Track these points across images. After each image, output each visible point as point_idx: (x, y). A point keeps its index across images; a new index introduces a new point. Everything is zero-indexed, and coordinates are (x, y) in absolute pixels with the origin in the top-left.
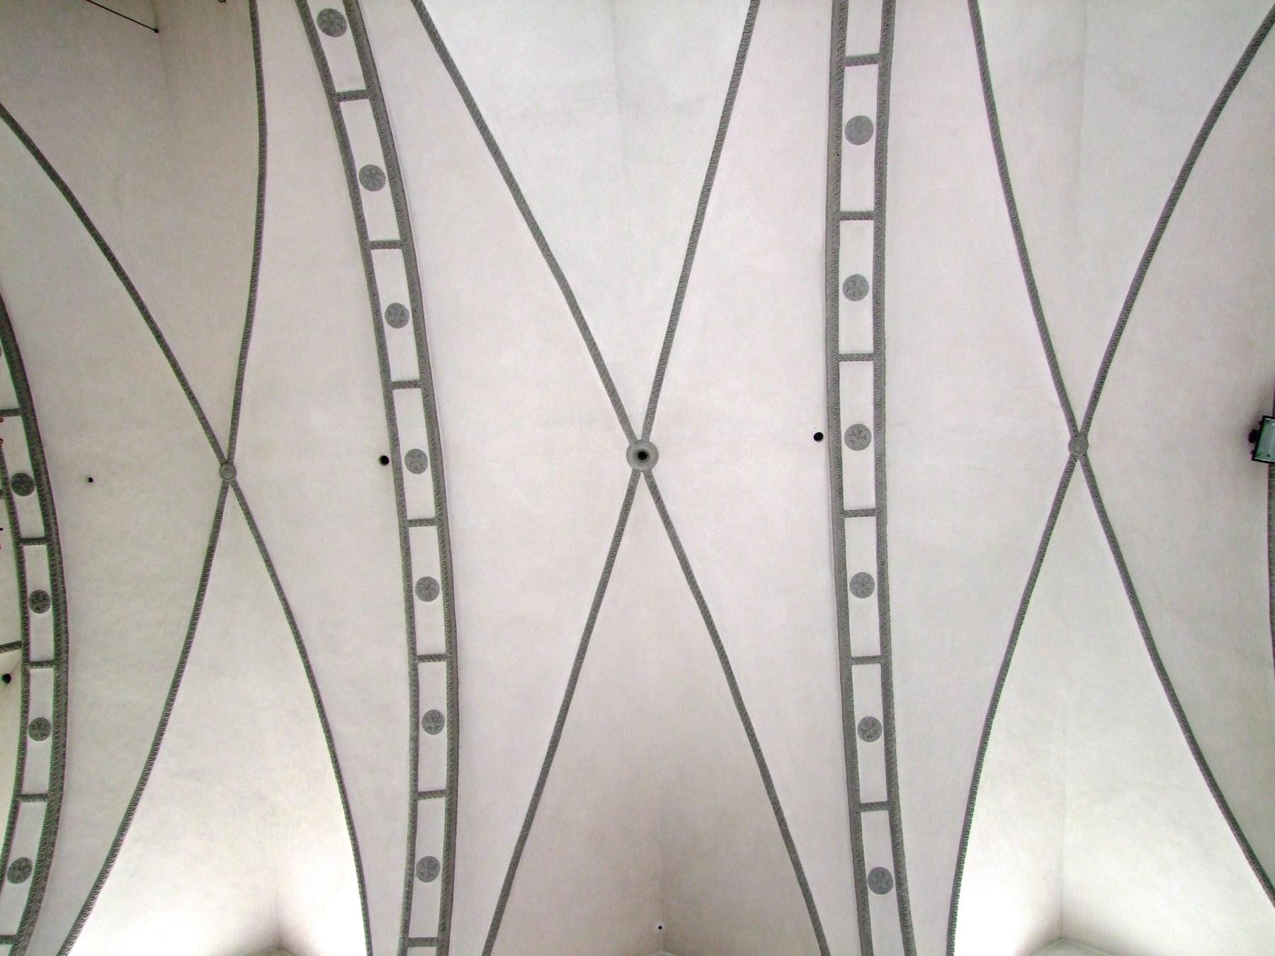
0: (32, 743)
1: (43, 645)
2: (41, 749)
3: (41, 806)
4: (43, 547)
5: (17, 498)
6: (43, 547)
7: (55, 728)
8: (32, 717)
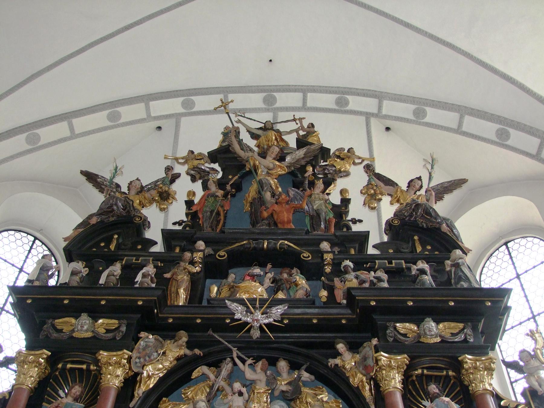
0: (427, 119)
1: (369, 105)
2: (432, 115)
3: (467, 119)
4: (309, 95)
5: (278, 105)
6: (309, 95)
7: (421, 105)
8: (411, 117)
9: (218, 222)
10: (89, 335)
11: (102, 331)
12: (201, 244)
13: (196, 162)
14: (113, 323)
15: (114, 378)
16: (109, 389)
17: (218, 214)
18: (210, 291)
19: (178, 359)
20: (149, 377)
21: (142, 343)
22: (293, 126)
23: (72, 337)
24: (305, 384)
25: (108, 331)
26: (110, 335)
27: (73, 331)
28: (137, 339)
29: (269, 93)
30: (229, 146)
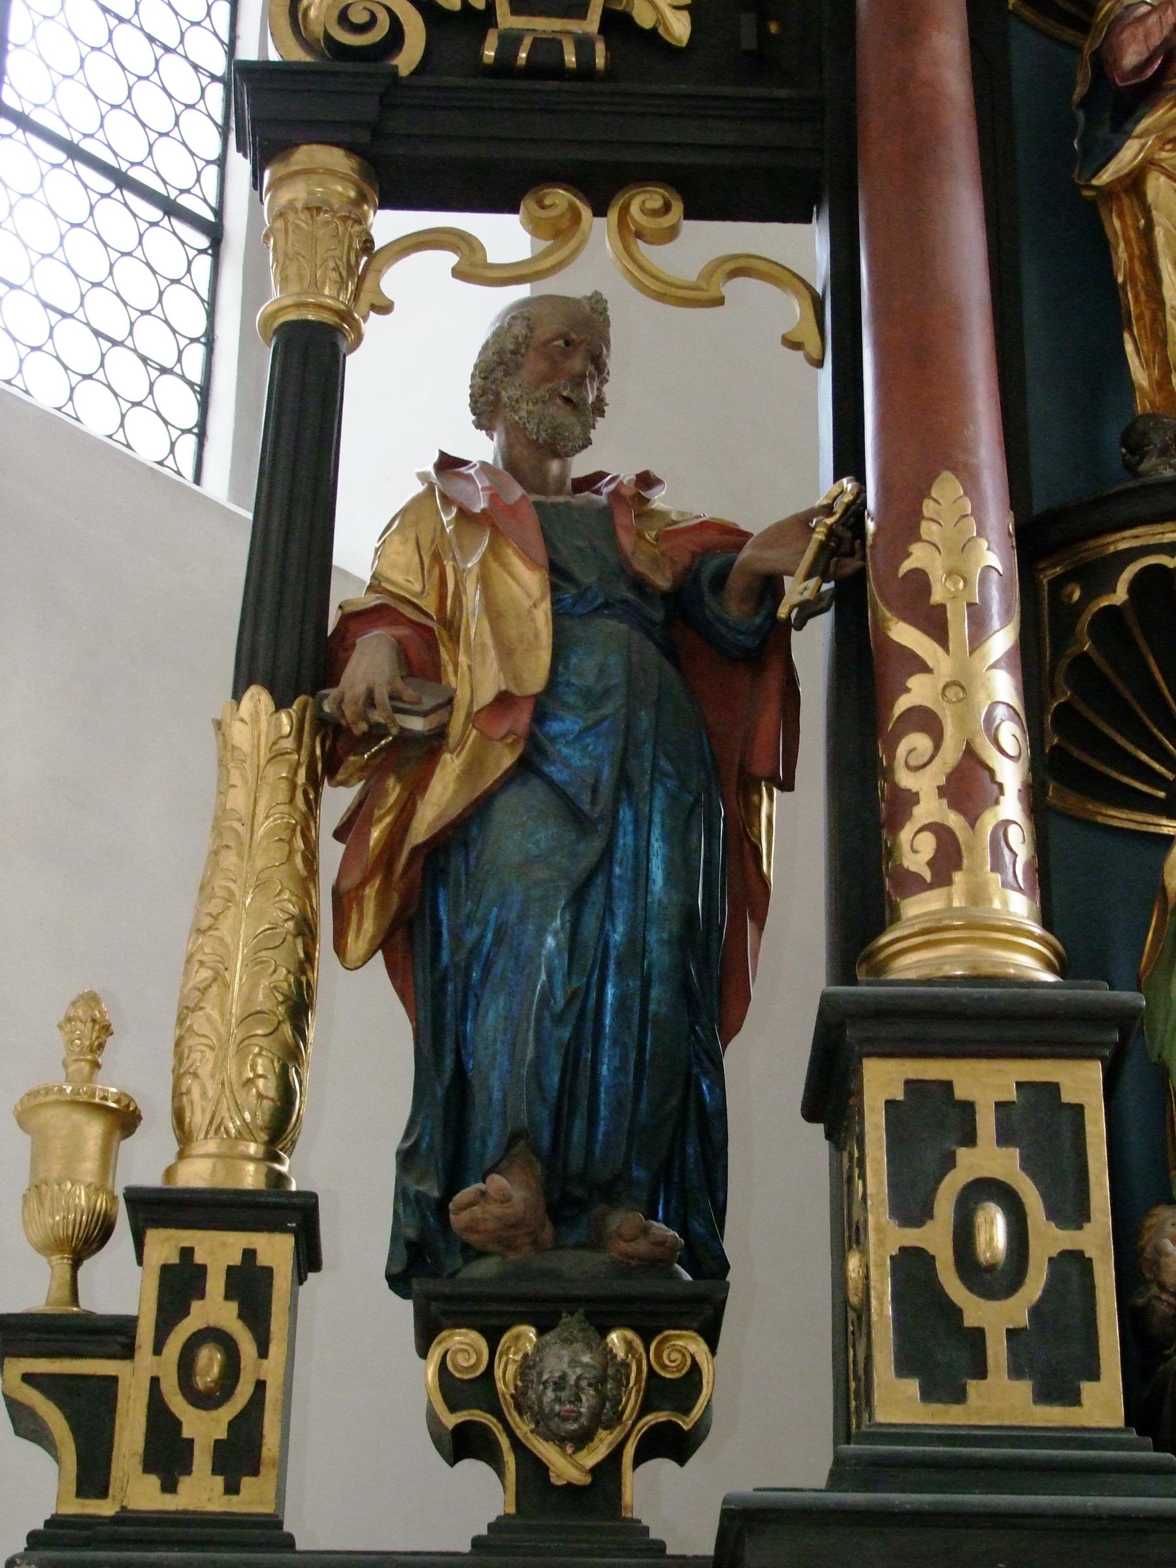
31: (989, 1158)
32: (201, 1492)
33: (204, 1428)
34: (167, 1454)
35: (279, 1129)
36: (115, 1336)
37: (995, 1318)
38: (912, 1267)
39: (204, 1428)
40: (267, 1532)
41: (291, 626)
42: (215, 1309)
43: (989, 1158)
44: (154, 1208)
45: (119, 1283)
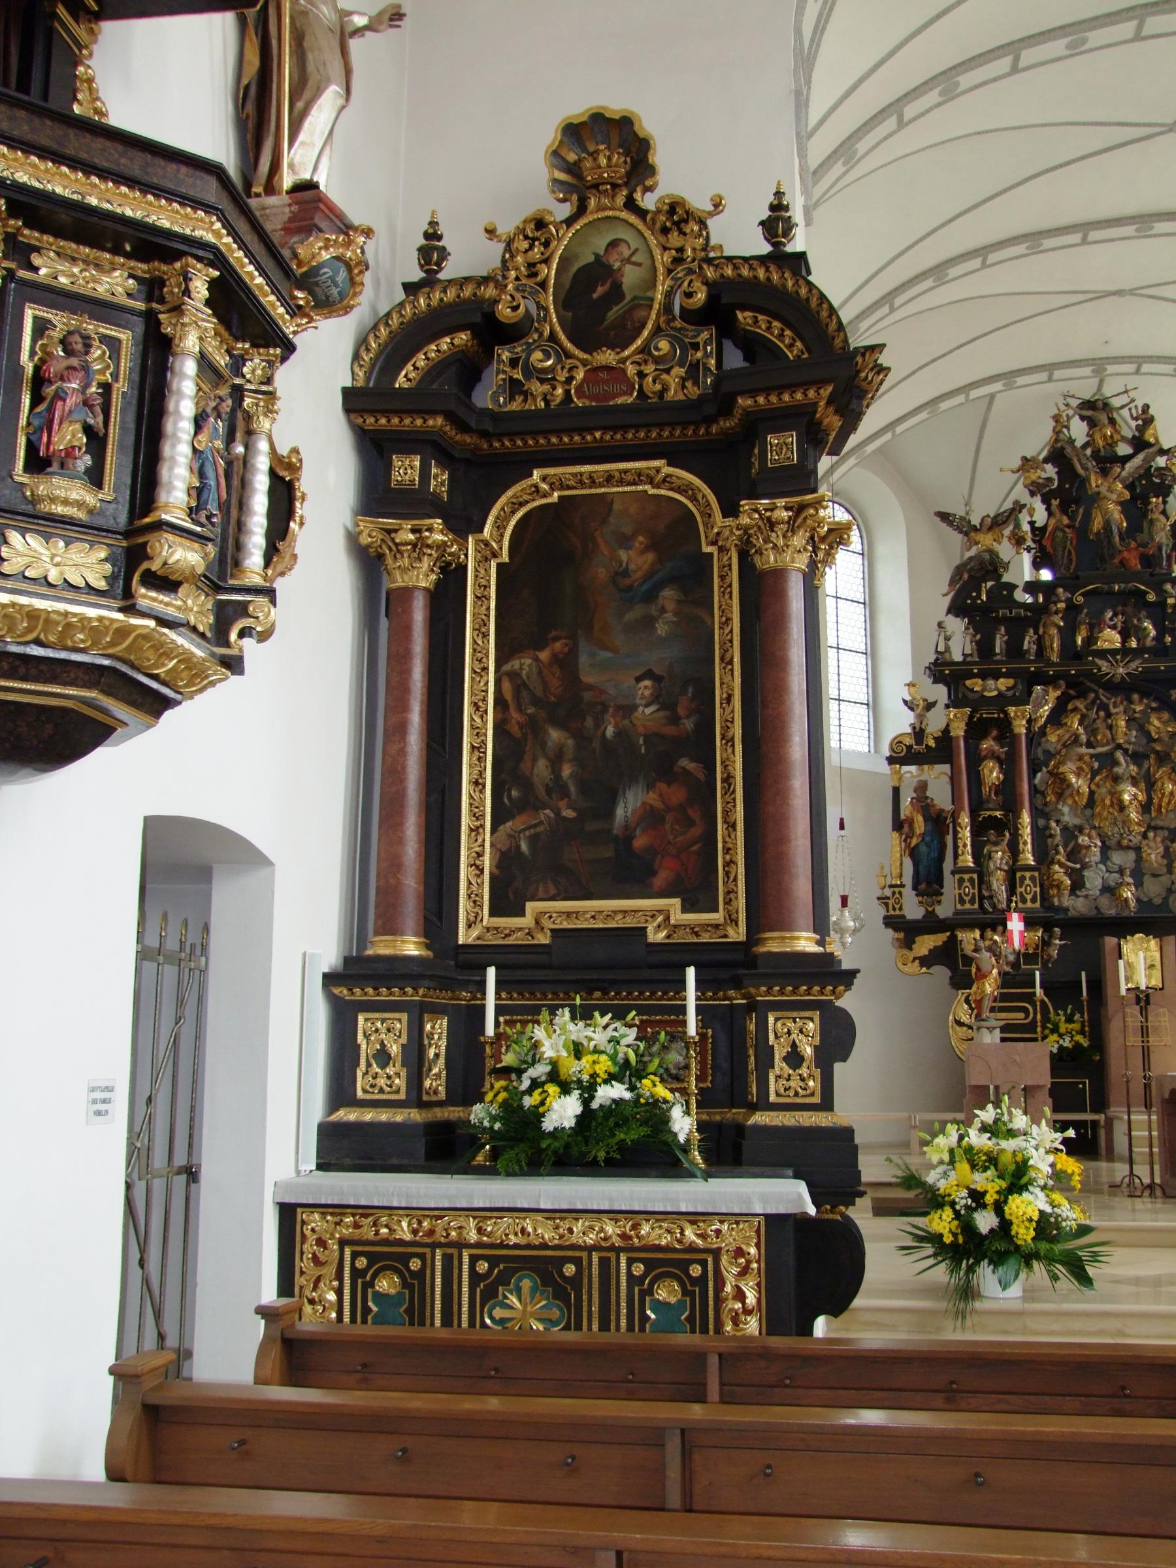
9: (1070, 560)
10: (995, 693)
11: (1004, 688)
12: (1061, 590)
13: (1034, 476)
14: (1011, 682)
15: (1020, 727)
16: (1019, 735)
17: (1070, 552)
18: (1075, 642)
19: (1058, 698)
20: (1041, 717)
21: (1034, 695)
22: (1124, 400)
23: (983, 696)
24: (1153, 709)
25: (1009, 689)
26: (1010, 693)
27: (984, 690)
28: (1030, 693)
29: (1099, 365)
30: (1063, 448)
31: (967, 884)
32: (897, 912)
33: (897, 907)
34: (894, 909)
35: (901, 876)
36: (888, 898)
37: (967, 899)
38: (960, 895)
39: (897, 907)
40: (904, 917)
41: (898, 824)
42: (897, 895)
43: (967, 884)
44: (891, 886)
45: (888, 892)
